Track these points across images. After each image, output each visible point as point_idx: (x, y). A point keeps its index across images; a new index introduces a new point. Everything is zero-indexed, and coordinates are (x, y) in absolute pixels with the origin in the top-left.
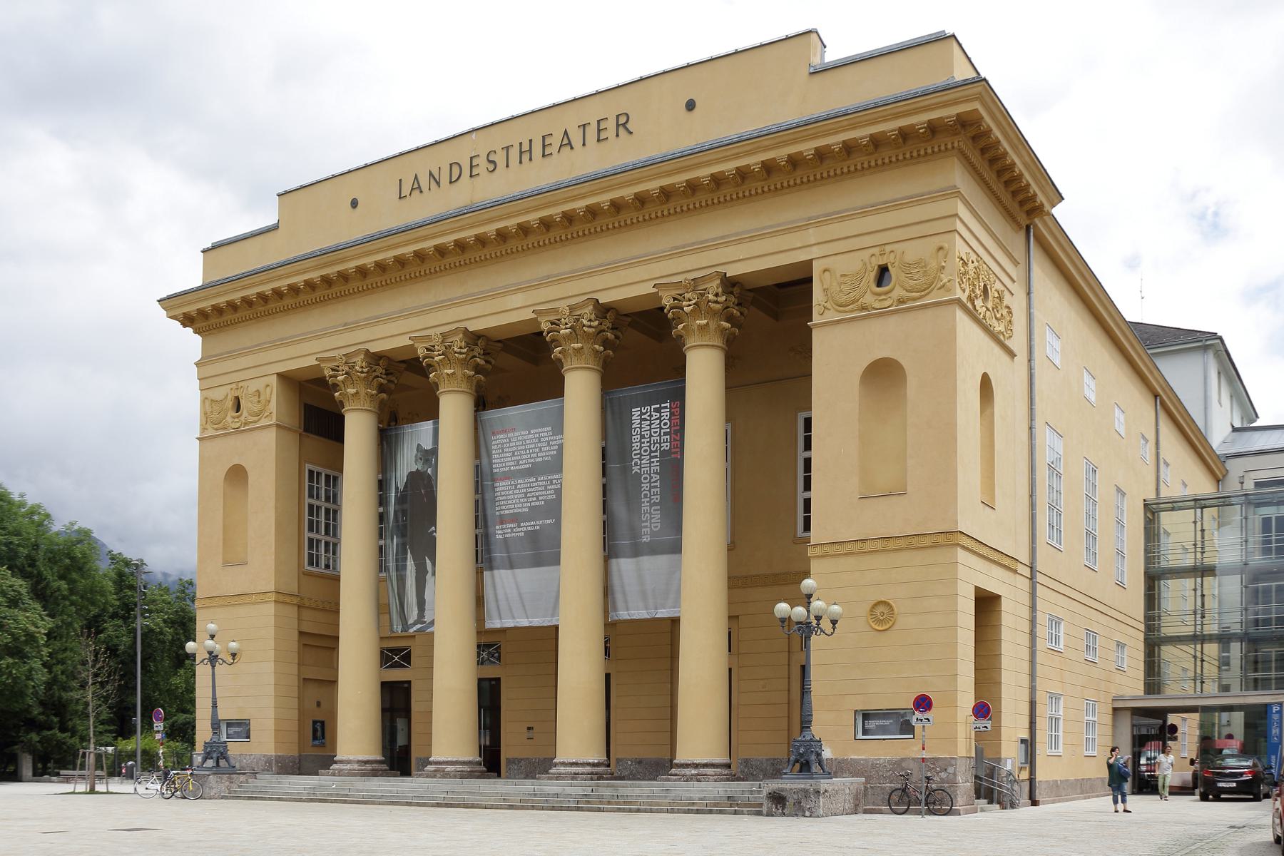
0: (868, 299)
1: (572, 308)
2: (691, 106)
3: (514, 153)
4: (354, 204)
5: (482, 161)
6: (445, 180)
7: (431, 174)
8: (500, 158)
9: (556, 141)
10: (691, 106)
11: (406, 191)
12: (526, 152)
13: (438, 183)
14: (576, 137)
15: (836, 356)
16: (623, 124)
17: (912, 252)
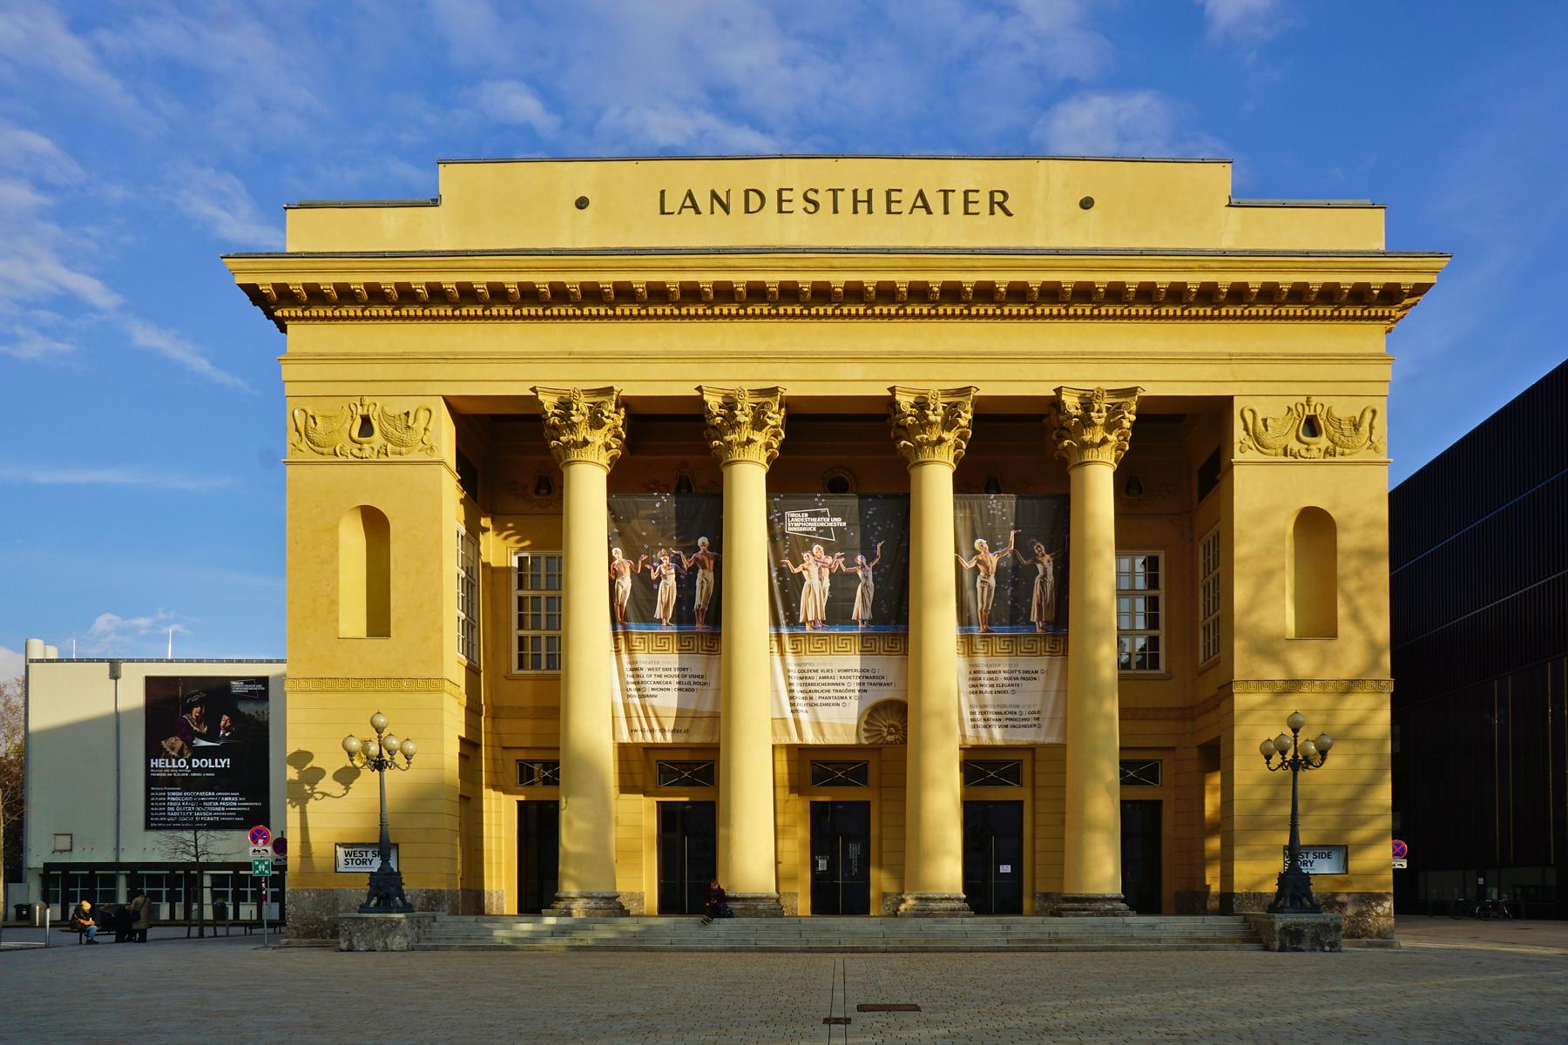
0: (1295, 446)
1: (947, 393)
2: (1087, 204)
3: (845, 200)
4: (582, 203)
5: (797, 196)
6: (737, 203)
7: (714, 195)
8: (825, 199)
9: (908, 197)
10: (1087, 204)
11: (672, 204)
12: (862, 202)
13: (726, 209)
14: (935, 202)
15: (1262, 496)
16: (999, 203)
17: (1344, 409)
